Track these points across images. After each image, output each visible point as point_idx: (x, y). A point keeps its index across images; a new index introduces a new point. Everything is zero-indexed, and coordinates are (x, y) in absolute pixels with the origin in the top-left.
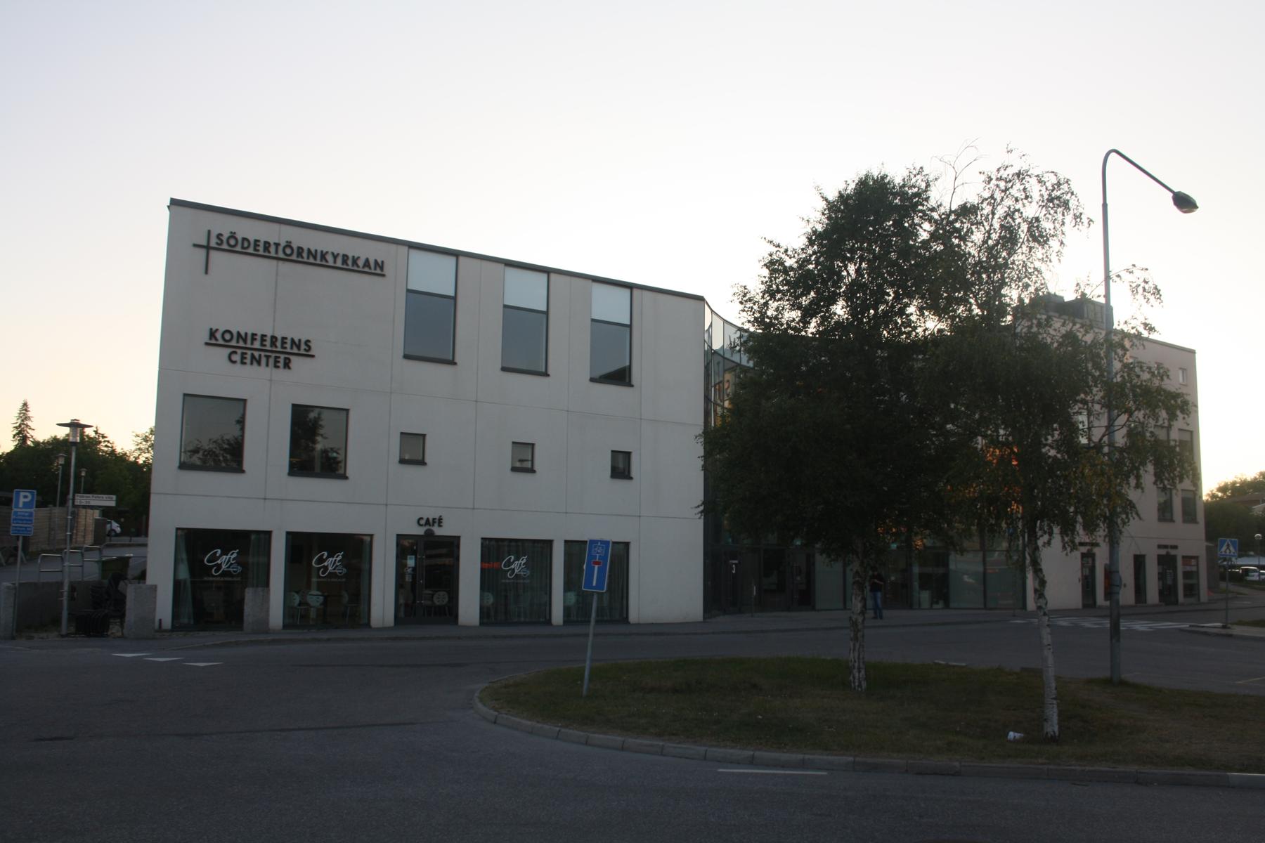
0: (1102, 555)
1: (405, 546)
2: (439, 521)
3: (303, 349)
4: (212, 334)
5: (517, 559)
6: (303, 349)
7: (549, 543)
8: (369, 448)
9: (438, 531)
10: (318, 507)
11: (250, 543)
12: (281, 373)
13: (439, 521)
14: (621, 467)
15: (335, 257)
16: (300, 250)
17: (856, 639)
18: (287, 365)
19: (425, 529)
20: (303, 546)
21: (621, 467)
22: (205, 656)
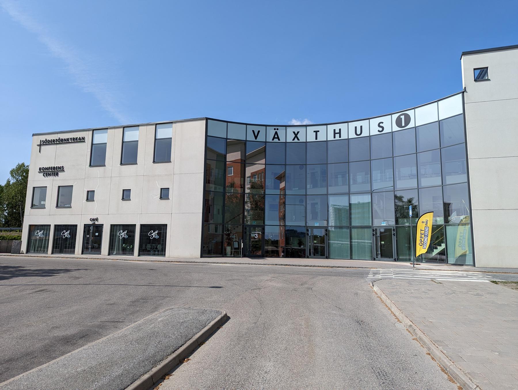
0: (28, 292)
1: (87, 227)
2: (97, 219)
3: (61, 169)
4: (40, 169)
5: (123, 232)
6: (61, 169)
7: (134, 226)
8: (78, 196)
9: (96, 223)
10: (64, 217)
11: (45, 228)
12: (56, 178)
13: (97, 219)
14: (164, 194)
15: (71, 139)
16: (62, 139)
17: (260, 289)
18: (57, 175)
19: (93, 222)
20: (59, 228)
21: (164, 194)
22: (90, 257)
